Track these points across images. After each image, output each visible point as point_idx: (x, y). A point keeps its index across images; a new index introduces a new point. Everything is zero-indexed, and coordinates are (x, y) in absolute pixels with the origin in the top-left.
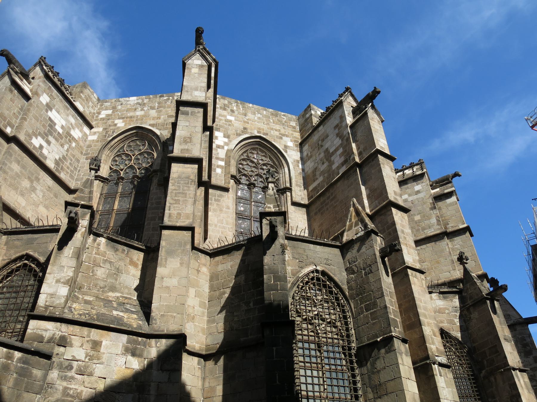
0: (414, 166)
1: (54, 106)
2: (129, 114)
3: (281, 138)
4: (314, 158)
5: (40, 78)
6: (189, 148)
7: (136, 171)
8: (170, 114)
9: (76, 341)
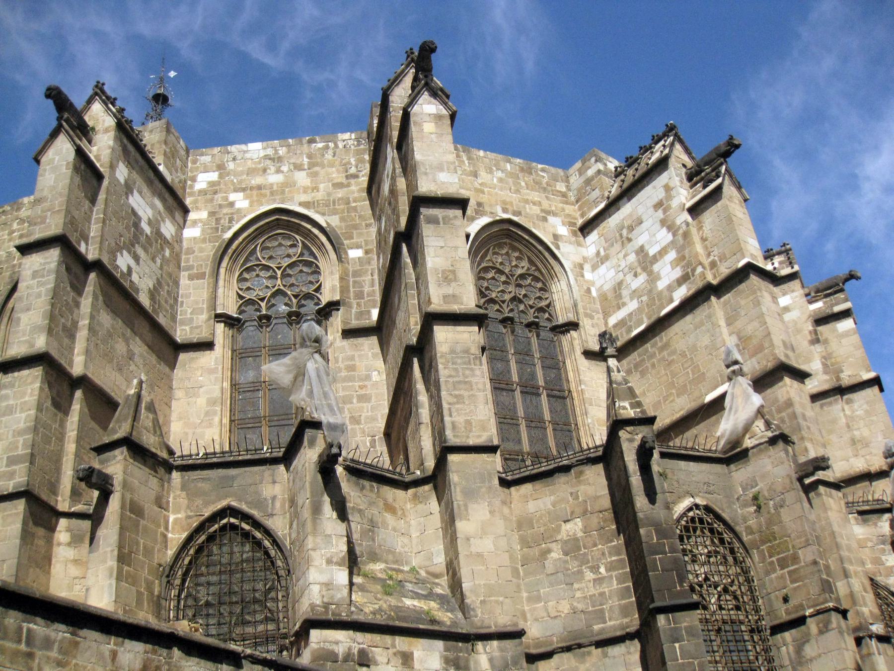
0: (774, 255)
1: (135, 183)
2: (257, 180)
3: (545, 219)
4: (614, 261)
5: (106, 131)
6: (457, 293)
7: (290, 299)
8: (336, 181)
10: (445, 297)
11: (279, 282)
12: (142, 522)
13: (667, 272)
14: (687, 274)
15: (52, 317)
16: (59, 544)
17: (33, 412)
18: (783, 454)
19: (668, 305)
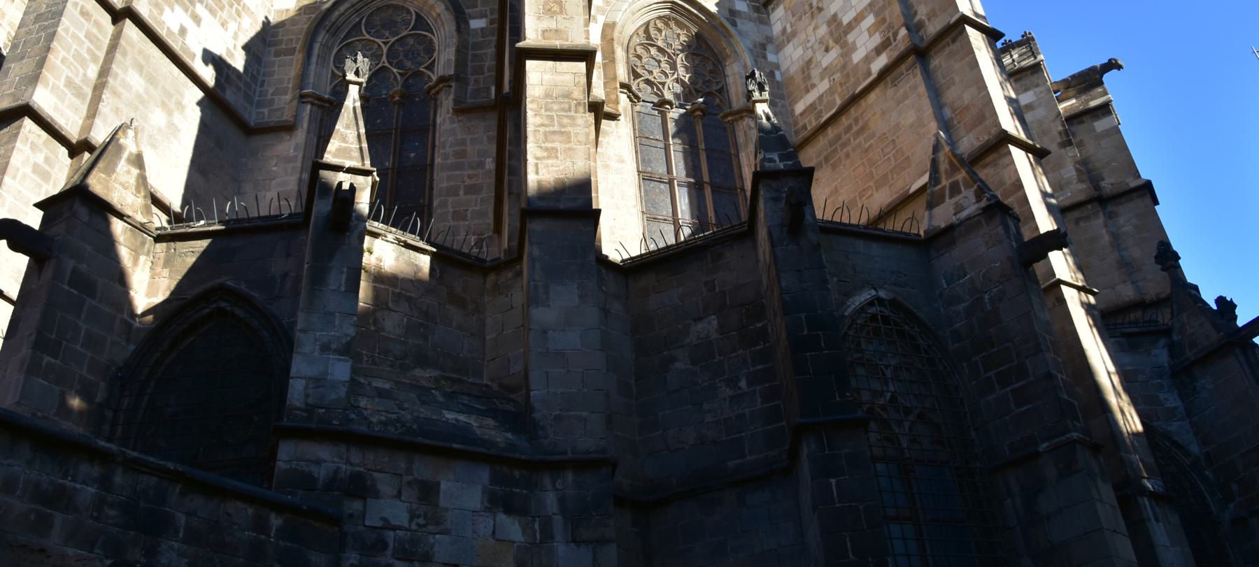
9: (385, 484)
10: (544, 32)
11: (384, 58)
12: (89, 301)
13: (864, 41)
14: (888, 38)
18: (1000, 230)
19: (865, 79)
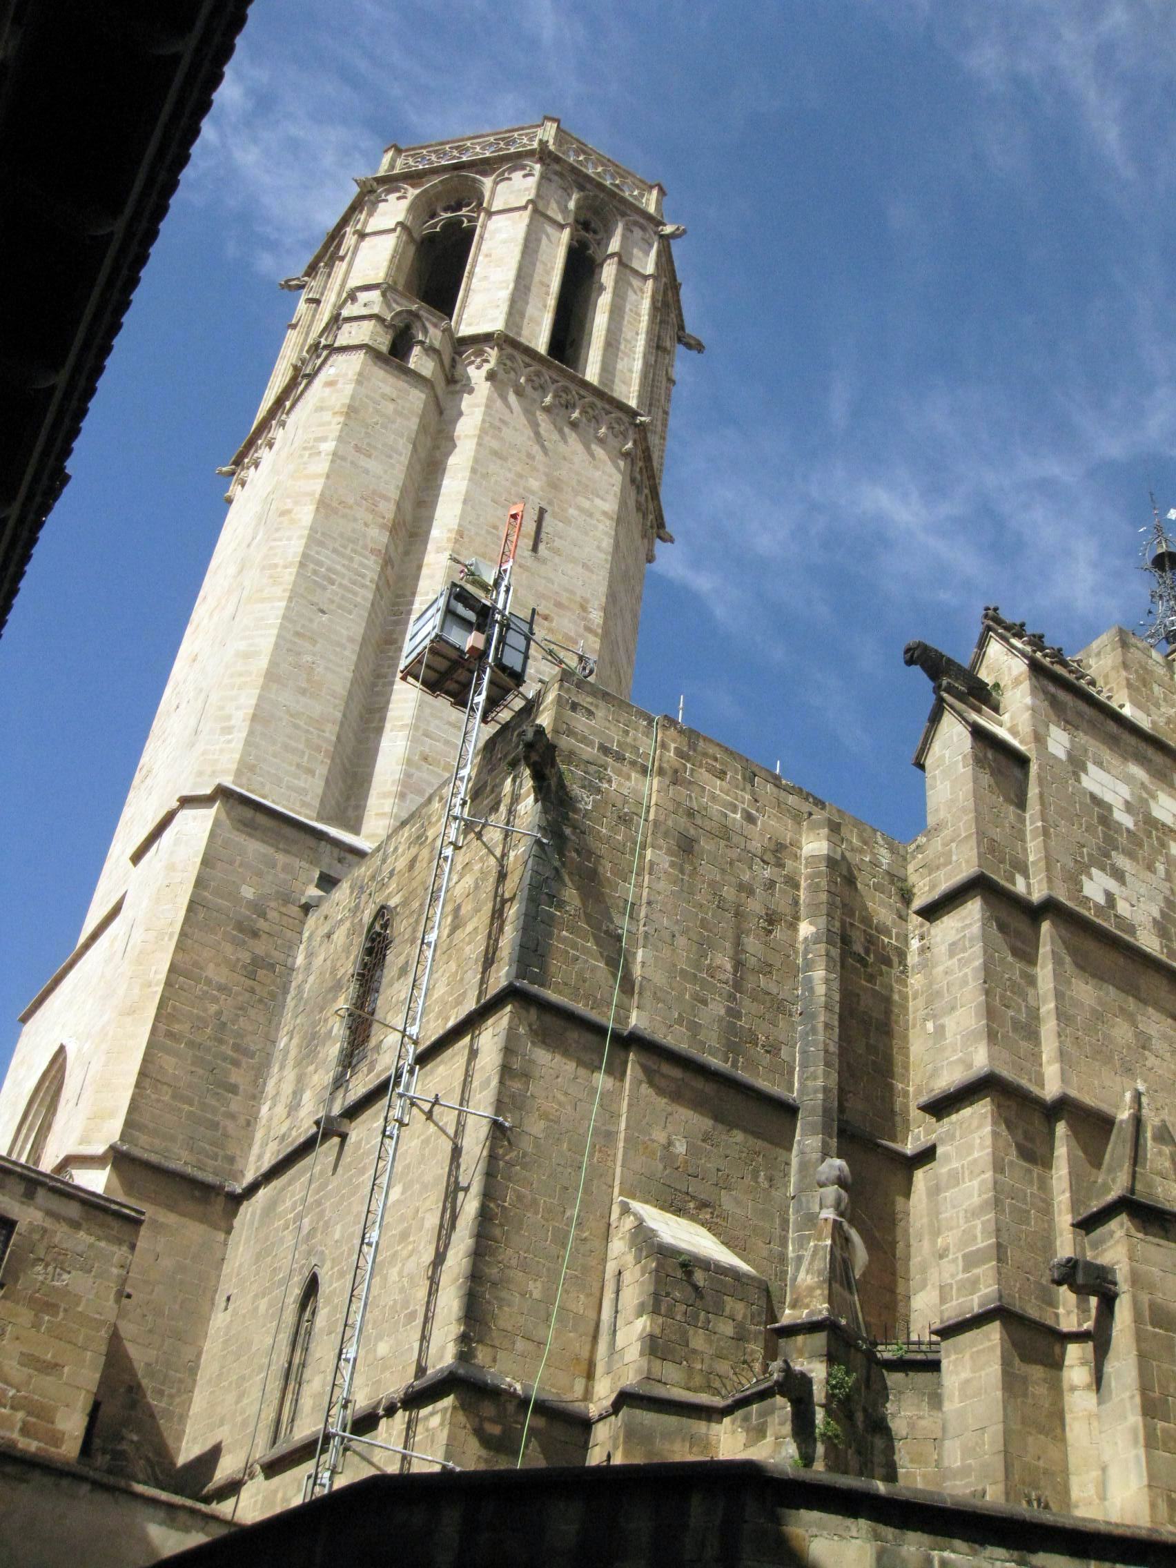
1: (1086, 751)
5: (1017, 682)
15: (991, 1013)
16: (1073, 1389)
17: (989, 1175)
